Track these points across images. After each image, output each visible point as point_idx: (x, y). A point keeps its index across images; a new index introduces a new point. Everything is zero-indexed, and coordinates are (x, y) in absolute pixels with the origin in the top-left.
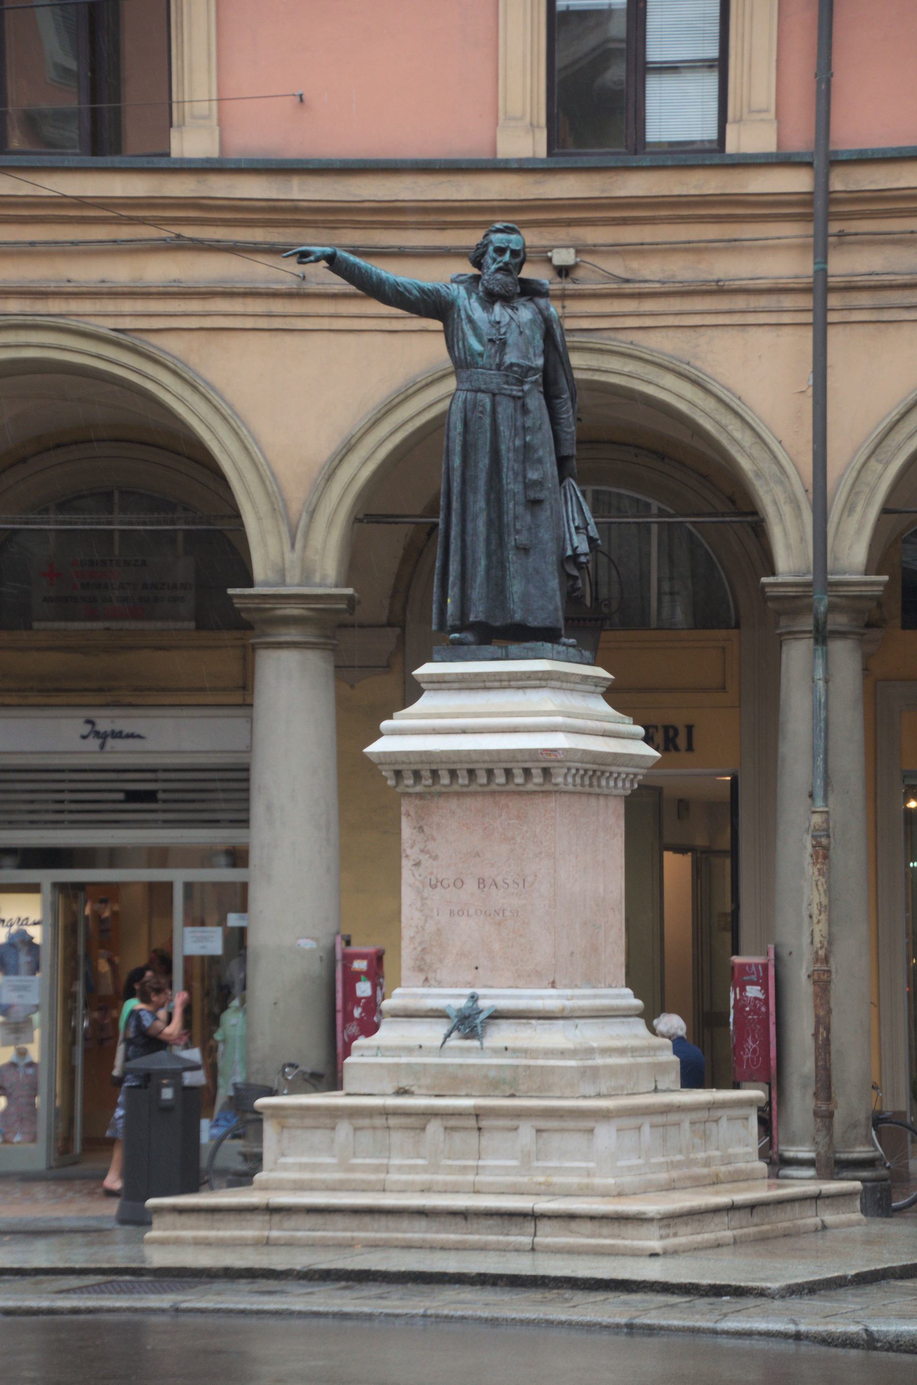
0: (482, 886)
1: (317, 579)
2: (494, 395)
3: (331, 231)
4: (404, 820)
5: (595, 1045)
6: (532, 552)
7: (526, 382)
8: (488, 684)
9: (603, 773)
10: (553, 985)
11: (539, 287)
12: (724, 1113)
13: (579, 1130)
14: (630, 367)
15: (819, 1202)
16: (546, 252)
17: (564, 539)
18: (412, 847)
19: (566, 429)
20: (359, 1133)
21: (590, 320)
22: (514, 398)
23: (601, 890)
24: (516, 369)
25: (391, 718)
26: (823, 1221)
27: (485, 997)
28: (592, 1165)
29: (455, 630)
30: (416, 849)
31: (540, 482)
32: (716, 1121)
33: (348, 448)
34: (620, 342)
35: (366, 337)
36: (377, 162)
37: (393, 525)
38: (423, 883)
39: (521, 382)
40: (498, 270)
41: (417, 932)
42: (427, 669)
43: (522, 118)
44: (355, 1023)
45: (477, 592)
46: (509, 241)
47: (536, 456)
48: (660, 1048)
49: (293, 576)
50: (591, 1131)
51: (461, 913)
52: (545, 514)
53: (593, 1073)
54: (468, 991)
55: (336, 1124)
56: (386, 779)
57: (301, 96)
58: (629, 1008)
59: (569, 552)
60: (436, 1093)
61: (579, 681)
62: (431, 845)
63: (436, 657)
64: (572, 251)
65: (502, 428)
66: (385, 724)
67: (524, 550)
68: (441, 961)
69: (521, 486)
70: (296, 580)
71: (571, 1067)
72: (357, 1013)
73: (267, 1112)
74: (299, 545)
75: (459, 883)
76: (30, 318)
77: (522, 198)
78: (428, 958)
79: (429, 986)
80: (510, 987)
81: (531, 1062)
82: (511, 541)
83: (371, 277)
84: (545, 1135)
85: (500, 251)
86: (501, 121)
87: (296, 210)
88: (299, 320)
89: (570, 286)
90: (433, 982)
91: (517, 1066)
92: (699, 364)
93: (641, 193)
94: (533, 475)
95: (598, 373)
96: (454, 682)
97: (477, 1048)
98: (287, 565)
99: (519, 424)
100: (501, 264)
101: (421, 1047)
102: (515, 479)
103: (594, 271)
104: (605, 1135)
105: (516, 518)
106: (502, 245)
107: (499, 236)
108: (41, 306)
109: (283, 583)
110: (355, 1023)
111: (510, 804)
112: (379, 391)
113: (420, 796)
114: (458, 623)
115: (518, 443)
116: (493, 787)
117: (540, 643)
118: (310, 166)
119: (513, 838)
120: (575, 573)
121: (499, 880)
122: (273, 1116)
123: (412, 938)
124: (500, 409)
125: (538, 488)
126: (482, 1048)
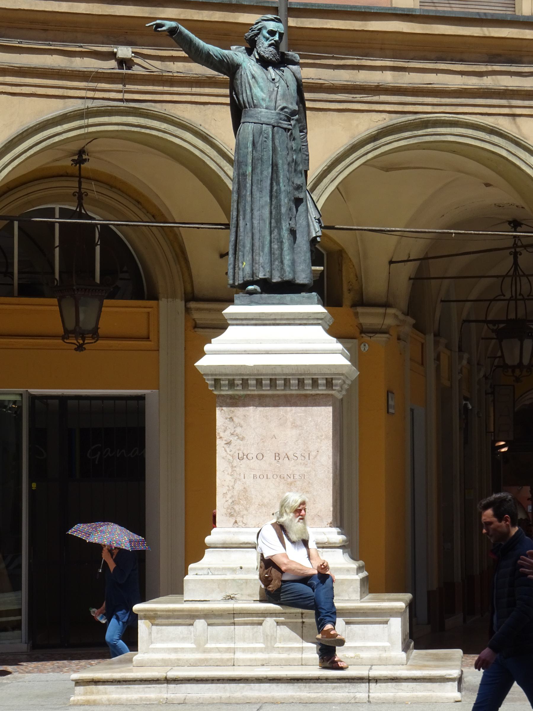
2: (274, 127)
7: (293, 119)
14: (164, 126)
18: (225, 431)
22: (285, 129)
25: (210, 342)
30: (228, 432)
39: (289, 120)
40: (270, 45)
42: (231, 310)
51: (261, 477)
62: (238, 430)
63: (236, 301)
65: (279, 149)
66: (207, 347)
69: (291, 188)
78: (237, 508)
79: (237, 527)
85: (272, 33)
90: (240, 524)
92: (207, 127)
100: (273, 41)
101: (241, 568)
106: (274, 29)
115: (289, 159)
121: (290, 454)
123: (225, 494)
124: (277, 136)
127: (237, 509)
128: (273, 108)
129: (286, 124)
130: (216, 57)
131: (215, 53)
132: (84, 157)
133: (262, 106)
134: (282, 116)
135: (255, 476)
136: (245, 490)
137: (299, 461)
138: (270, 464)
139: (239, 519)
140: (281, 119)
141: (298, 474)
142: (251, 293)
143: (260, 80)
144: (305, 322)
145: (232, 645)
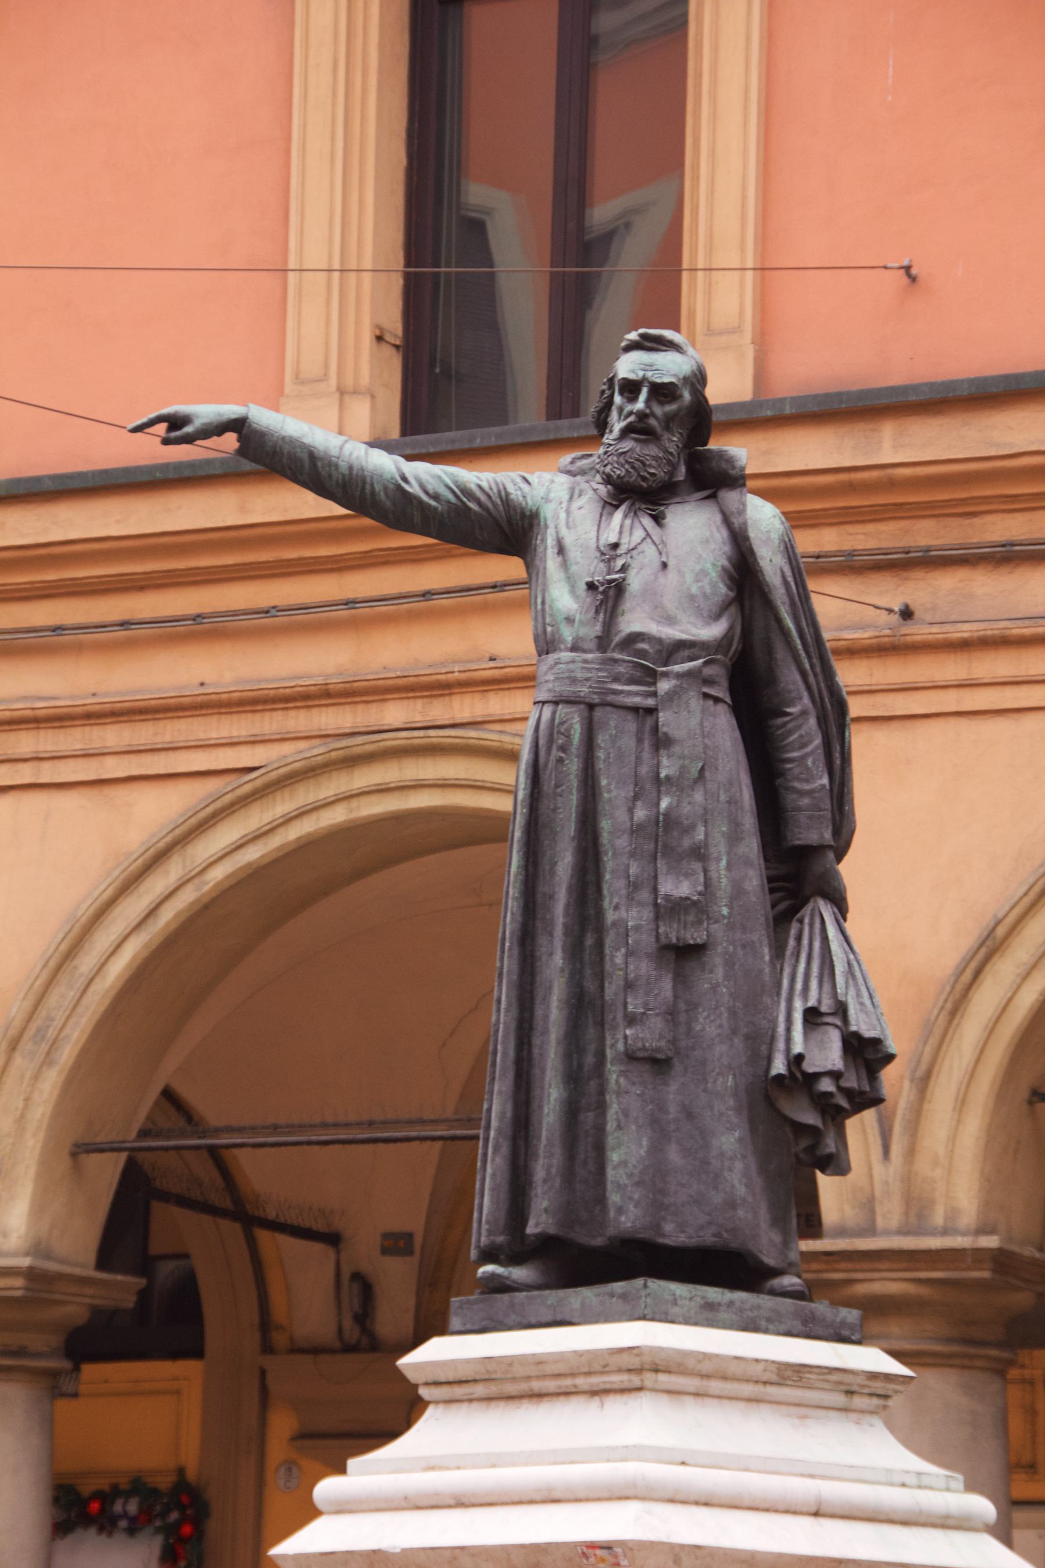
1: (938, 1218)
2: (591, 707)
3: (967, 522)
6: (678, 1066)
7: (665, 675)
8: (536, 1385)
11: (724, 465)
17: (773, 1039)
19: (797, 785)
22: (635, 710)
29: (489, 1255)
39: (650, 676)
40: (625, 432)
45: (546, 1165)
47: (687, 843)
52: (714, 975)
57: (907, 269)
59: (779, 1066)
61: (774, 1378)
63: (455, 1322)
65: (604, 782)
67: (658, 1064)
69: (647, 914)
76: (421, 733)
83: (337, 466)
85: (630, 388)
87: (892, 485)
94: (677, 887)
96: (475, 1381)
98: (877, 1194)
99: (644, 770)
100: (632, 419)
102: (630, 897)
105: (629, 986)
106: (632, 376)
108: (439, 711)
109: (870, 1230)
114: (500, 1239)
115: (641, 813)
117: (639, 1282)
118: (913, 398)
120: (810, 1118)
124: (602, 739)
125: (691, 918)
128: (592, 645)
129: (637, 694)
130: (436, 497)
131: (430, 488)
133: (563, 641)
134: (621, 669)
140: (616, 680)
142: (498, 1287)
143: (574, 553)
144: (596, 1381)
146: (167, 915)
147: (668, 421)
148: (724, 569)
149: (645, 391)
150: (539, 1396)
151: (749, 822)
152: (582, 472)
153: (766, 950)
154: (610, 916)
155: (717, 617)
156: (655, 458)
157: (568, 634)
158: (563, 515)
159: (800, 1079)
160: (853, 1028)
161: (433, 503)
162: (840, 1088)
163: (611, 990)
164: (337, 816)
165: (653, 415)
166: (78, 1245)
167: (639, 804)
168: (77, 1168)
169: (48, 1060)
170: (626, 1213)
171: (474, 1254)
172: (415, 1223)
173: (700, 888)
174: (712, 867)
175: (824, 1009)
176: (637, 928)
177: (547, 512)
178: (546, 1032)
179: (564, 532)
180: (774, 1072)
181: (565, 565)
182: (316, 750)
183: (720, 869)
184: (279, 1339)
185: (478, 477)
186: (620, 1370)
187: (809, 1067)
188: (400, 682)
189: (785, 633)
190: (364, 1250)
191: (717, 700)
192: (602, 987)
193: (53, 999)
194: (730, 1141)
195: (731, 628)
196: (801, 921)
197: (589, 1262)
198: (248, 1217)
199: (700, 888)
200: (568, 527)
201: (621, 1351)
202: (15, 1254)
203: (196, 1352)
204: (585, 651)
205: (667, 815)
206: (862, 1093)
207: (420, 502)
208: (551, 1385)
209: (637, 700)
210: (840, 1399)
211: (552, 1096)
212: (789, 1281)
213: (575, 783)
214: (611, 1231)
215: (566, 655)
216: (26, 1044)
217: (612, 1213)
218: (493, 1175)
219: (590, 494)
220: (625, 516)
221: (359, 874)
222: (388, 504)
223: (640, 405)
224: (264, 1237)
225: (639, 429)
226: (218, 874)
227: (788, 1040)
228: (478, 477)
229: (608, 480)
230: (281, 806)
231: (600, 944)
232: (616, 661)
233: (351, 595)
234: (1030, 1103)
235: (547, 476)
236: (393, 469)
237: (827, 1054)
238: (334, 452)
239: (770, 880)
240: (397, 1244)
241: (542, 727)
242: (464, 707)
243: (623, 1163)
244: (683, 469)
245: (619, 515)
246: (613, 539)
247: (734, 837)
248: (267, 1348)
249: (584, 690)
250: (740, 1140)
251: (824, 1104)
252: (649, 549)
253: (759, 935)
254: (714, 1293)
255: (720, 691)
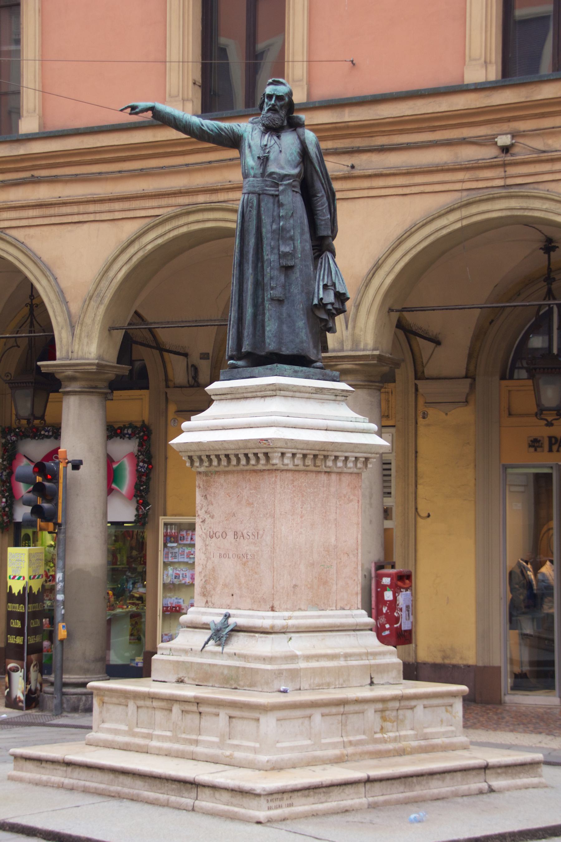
0: (236, 537)
1: (362, 346)
2: (259, 195)
3: (370, 139)
4: (197, 490)
5: (298, 653)
6: (286, 302)
7: (281, 185)
8: (245, 395)
9: (336, 458)
10: (273, 609)
11: (298, 121)
12: (419, 705)
13: (252, 719)
14: (547, 205)
15: (487, 771)
16: (494, 138)
17: (314, 293)
18: (201, 509)
19: (320, 218)
20: (140, 710)
21: (521, 178)
22: (272, 195)
23: (333, 540)
24: (275, 176)
25: (190, 420)
26: (490, 786)
27: (234, 616)
28: (257, 745)
29: (231, 358)
30: (203, 510)
31: (291, 253)
32: (412, 708)
33: (377, 267)
34: (541, 191)
35: (389, 199)
36: (391, 94)
37: (411, 312)
38: (206, 534)
39: (277, 185)
40: (269, 110)
41: (203, 569)
42: (216, 386)
43: (480, 59)
44: (384, 616)
45: (247, 331)
46: (276, 90)
47: (288, 235)
48: (383, 654)
49: (348, 345)
50: (258, 720)
51: (225, 556)
52: (296, 274)
53: (294, 674)
54: (224, 611)
55: (128, 703)
56: (185, 462)
57: (352, 61)
58: (366, 624)
59: (316, 302)
60: (197, 683)
61: (314, 392)
62: (211, 507)
64: (509, 136)
65: (263, 217)
66: (185, 425)
67: (280, 301)
68: (214, 589)
70: (349, 347)
71: (268, 670)
72: (385, 610)
73: (95, 692)
74: (350, 326)
75: (224, 535)
76: (209, 204)
77: (478, 106)
78: (208, 587)
79: (208, 607)
80: (250, 609)
81: (248, 665)
82: (267, 296)
83: (182, 121)
84: (234, 720)
85: (270, 97)
86: (467, 63)
87: (348, 128)
88: (351, 193)
89: (509, 158)
90: (210, 604)
91: (239, 667)
93: (551, 96)
94: (285, 249)
95: (527, 211)
97: (220, 653)
98: (344, 339)
99: (275, 214)
100: (270, 106)
102: (272, 252)
103: (524, 148)
104: (268, 723)
105: (271, 278)
106: (270, 93)
107: (271, 87)
109: (342, 350)
110: (384, 616)
111: (251, 479)
112: (395, 230)
113: (206, 474)
114: (234, 353)
115: (274, 227)
116: (241, 467)
117: (275, 365)
118: (354, 101)
119: (253, 504)
120: (325, 317)
121: (245, 532)
122: (98, 695)
123: (200, 573)
124: (262, 204)
125: (289, 258)
126: (222, 653)
127: (208, 589)
128: (259, 176)
129: (273, 190)
130: (212, 131)
132: (553, 244)
134: (268, 183)
135: (220, 555)
136: (214, 569)
137: (251, 540)
138: (231, 543)
139: (209, 599)
140: (267, 186)
141: (250, 554)
142: (234, 367)
143: (254, 148)
145: (150, 731)
146: (135, 260)
147: (281, 107)
148: (298, 152)
149: (274, 98)
150: (246, 398)
151: (307, 229)
152: (256, 123)
153: (312, 267)
154: (266, 258)
155: (296, 167)
156: (279, 118)
157: (252, 172)
158: (250, 136)
159: (322, 305)
160: (337, 290)
161: (211, 133)
162: (333, 308)
163: (266, 280)
164: (184, 230)
165: (276, 105)
166: (111, 356)
167: (274, 224)
168: (110, 334)
169: (101, 303)
170: (271, 345)
171: (227, 358)
172: (209, 349)
173: (292, 249)
174: (296, 242)
175: (329, 284)
176: (274, 261)
177: (245, 135)
178: (247, 292)
179: (250, 141)
180: (314, 303)
181: (251, 151)
182: (178, 210)
183: (298, 243)
184: (171, 384)
185: (224, 125)
186: (270, 390)
187: (324, 302)
188: (202, 189)
189: (317, 171)
190: (195, 358)
191: (297, 192)
192: (263, 279)
193: (102, 284)
194: (301, 323)
195: (301, 170)
196: (322, 259)
197: (261, 359)
198: (161, 349)
199: (292, 249)
200: (252, 140)
201: (270, 384)
202: (93, 359)
203: (147, 388)
204: (257, 178)
205: (282, 227)
206: (340, 309)
207: (207, 132)
208: (250, 395)
209: (273, 192)
210: (334, 398)
211: (249, 311)
212: (319, 364)
213: (255, 218)
214: (267, 350)
215: (252, 179)
216: (94, 298)
217: (267, 345)
218: (232, 335)
219: (258, 130)
220: (269, 136)
221: (191, 247)
222: (198, 133)
223: (273, 102)
224: (166, 354)
225: (273, 109)
226: (149, 247)
227: (318, 294)
228: (224, 125)
229: (263, 125)
230: (168, 227)
231: (263, 266)
232: (266, 181)
233: (187, 163)
234: (388, 312)
235: (245, 124)
236: (199, 122)
237: (330, 298)
238: (181, 117)
239: (313, 246)
240: (204, 356)
241: (245, 201)
242: (222, 196)
243: (270, 331)
244: (286, 122)
245: (267, 136)
246: (265, 143)
247: (302, 234)
248: (167, 386)
249: (257, 189)
250: (304, 323)
251: (329, 312)
252: (276, 147)
253: (310, 263)
254: (297, 368)
255: (298, 189)
